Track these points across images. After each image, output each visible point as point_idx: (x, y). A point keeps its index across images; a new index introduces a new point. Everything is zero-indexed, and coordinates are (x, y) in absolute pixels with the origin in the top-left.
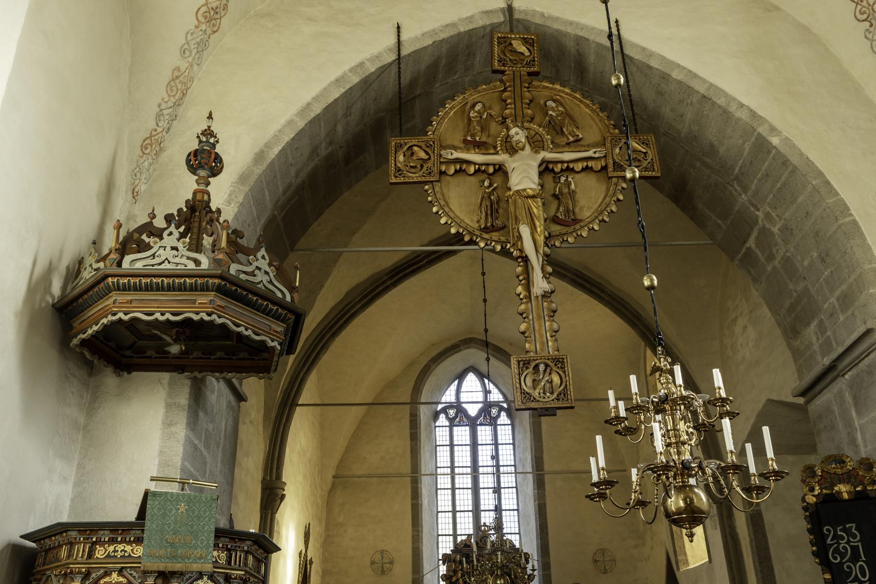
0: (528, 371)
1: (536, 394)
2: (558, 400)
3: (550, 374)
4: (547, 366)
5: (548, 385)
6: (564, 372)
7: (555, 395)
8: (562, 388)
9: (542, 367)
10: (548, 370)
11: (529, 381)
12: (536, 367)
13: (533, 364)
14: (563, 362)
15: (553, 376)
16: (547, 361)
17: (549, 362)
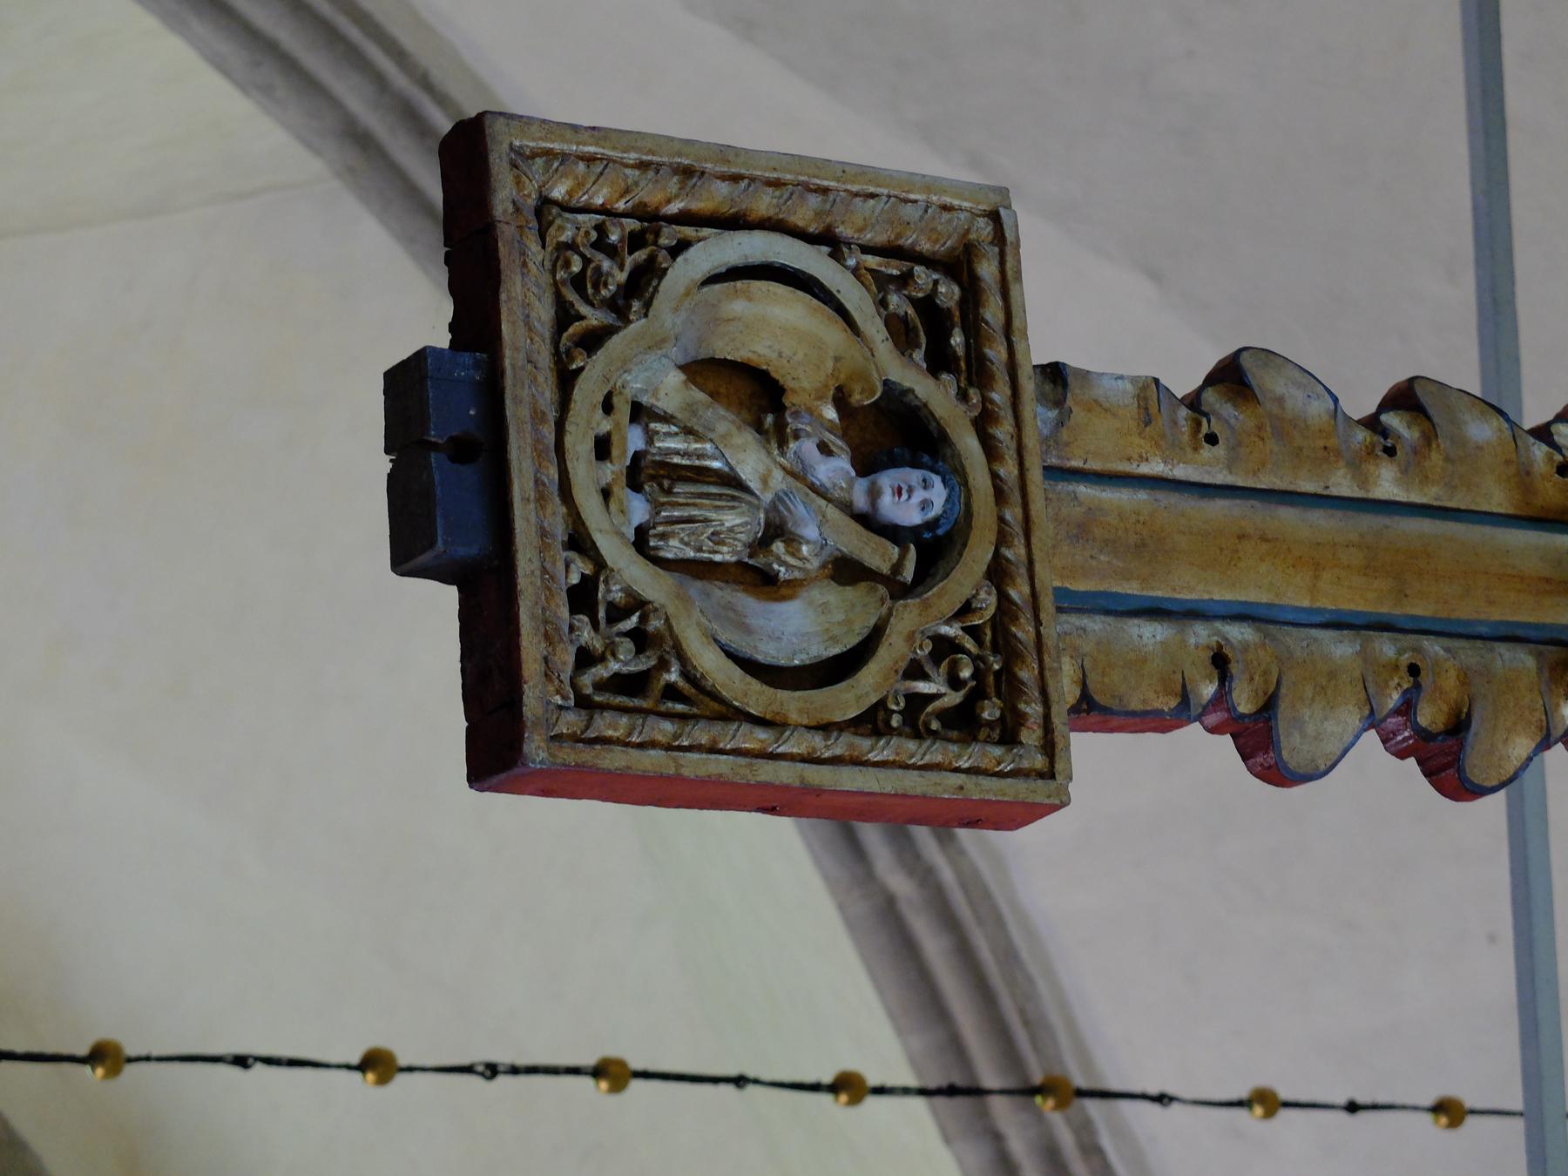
0: (874, 328)
1: (646, 364)
2: (582, 598)
3: (845, 570)
4: (935, 547)
5: (736, 523)
6: (872, 722)
7: (630, 572)
8: (710, 662)
9: (912, 498)
10: (878, 554)
11: (775, 328)
12: (891, 433)
13: (938, 397)
14: (963, 723)
15: (833, 596)
16: (978, 554)
17: (966, 577)
